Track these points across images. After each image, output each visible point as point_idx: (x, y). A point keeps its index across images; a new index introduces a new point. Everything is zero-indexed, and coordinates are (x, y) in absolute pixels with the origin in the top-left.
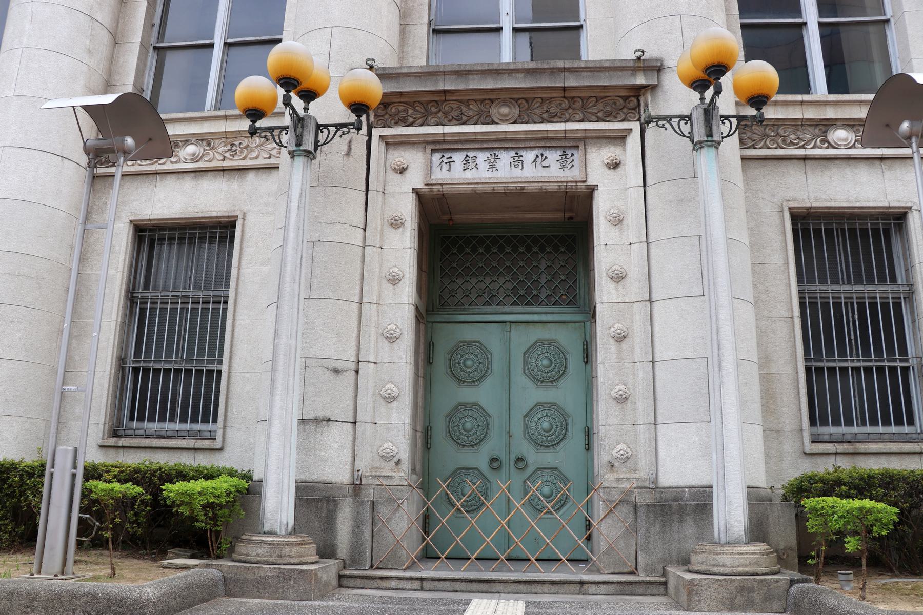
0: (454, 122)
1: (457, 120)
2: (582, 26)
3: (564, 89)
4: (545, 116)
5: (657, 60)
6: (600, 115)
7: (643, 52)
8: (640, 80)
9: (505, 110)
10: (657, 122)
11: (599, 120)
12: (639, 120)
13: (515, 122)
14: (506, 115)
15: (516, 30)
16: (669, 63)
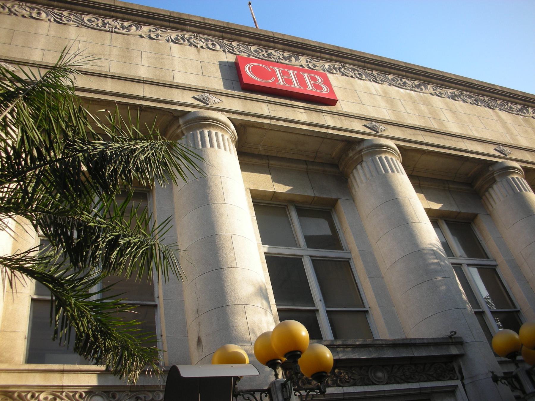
0: (347, 384)
1: (348, 382)
2: (367, 311)
3: (411, 358)
4: (403, 377)
5: (461, 338)
6: (435, 375)
7: (455, 333)
8: (454, 351)
9: (380, 374)
10: (501, 381)
11: (438, 380)
12: (458, 379)
13: (387, 384)
14: (380, 378)
15: (328, 312)
16: (466, 339)
